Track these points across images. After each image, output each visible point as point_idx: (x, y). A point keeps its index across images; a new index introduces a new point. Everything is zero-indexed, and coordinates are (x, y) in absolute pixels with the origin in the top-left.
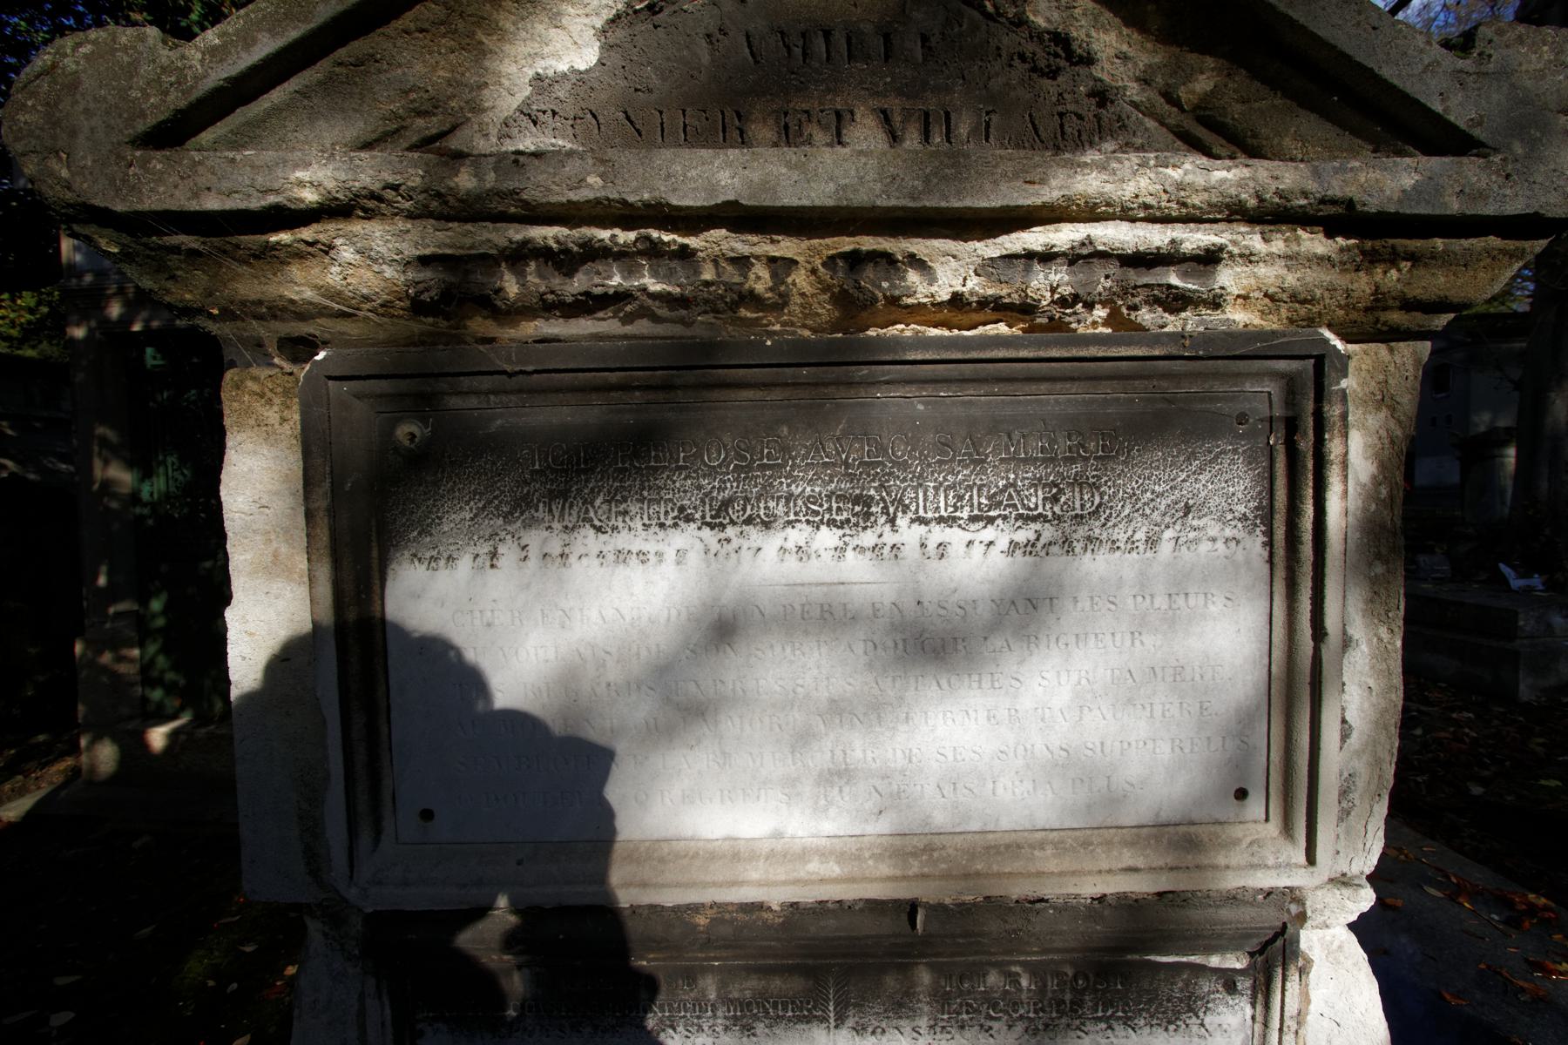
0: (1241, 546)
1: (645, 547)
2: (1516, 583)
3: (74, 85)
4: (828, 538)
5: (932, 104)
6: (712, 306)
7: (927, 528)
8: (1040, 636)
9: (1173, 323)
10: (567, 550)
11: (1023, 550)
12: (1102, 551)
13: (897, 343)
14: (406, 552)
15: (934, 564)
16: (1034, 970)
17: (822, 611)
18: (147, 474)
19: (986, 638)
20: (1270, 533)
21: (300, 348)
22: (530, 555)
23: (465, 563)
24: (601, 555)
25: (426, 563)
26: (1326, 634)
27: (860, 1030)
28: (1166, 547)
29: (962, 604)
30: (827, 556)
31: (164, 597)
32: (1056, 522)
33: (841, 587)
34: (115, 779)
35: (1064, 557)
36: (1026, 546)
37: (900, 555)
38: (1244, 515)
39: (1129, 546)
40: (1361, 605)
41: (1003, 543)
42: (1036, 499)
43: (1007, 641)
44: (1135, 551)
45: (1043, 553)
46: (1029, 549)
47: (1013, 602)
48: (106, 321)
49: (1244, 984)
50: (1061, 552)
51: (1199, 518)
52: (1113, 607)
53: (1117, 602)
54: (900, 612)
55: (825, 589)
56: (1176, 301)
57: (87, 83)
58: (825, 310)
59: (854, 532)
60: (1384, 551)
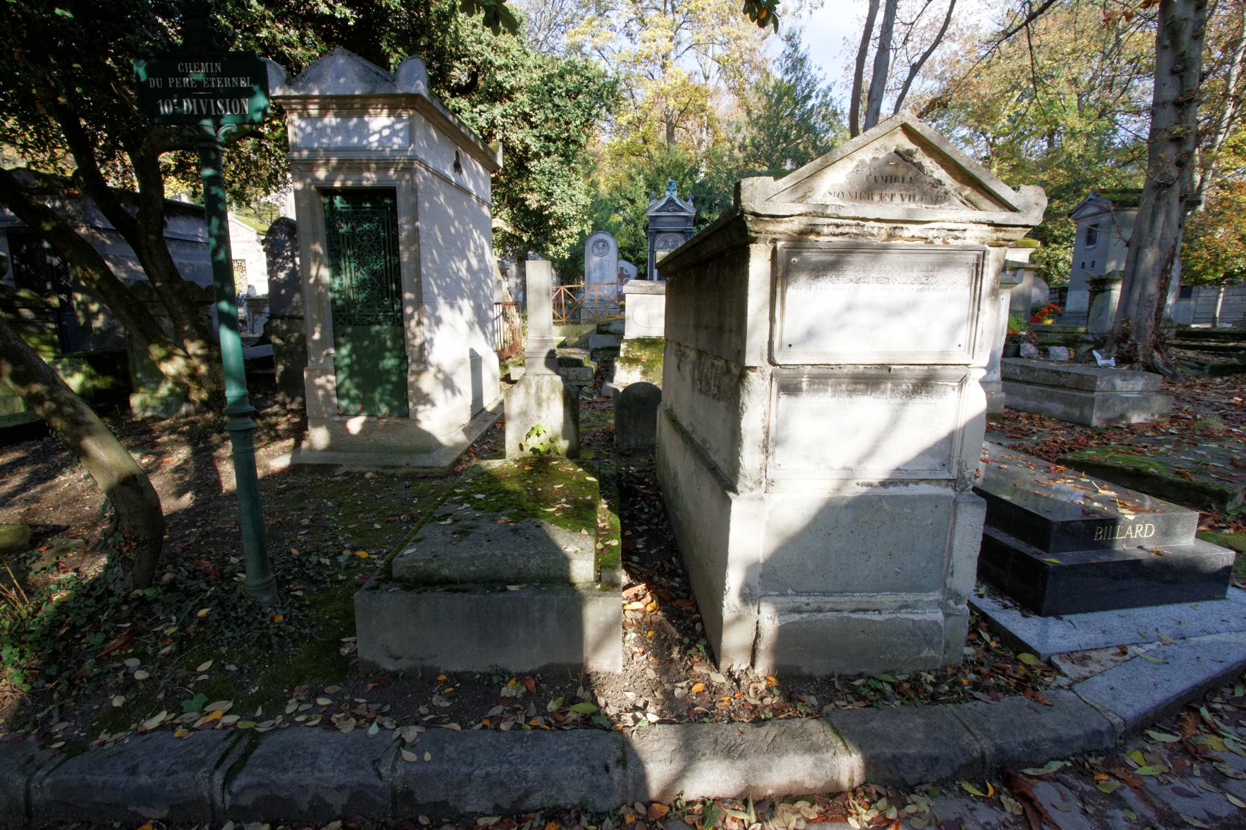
2: (1101, 362)
3: (756, 189)
5: (911, 192)
13: (897, 245)
18: (336, 271)
31: (349, 346)
34: (330, 448)
49: (957, 389)
56: (957, 238)
57: (759, 188)
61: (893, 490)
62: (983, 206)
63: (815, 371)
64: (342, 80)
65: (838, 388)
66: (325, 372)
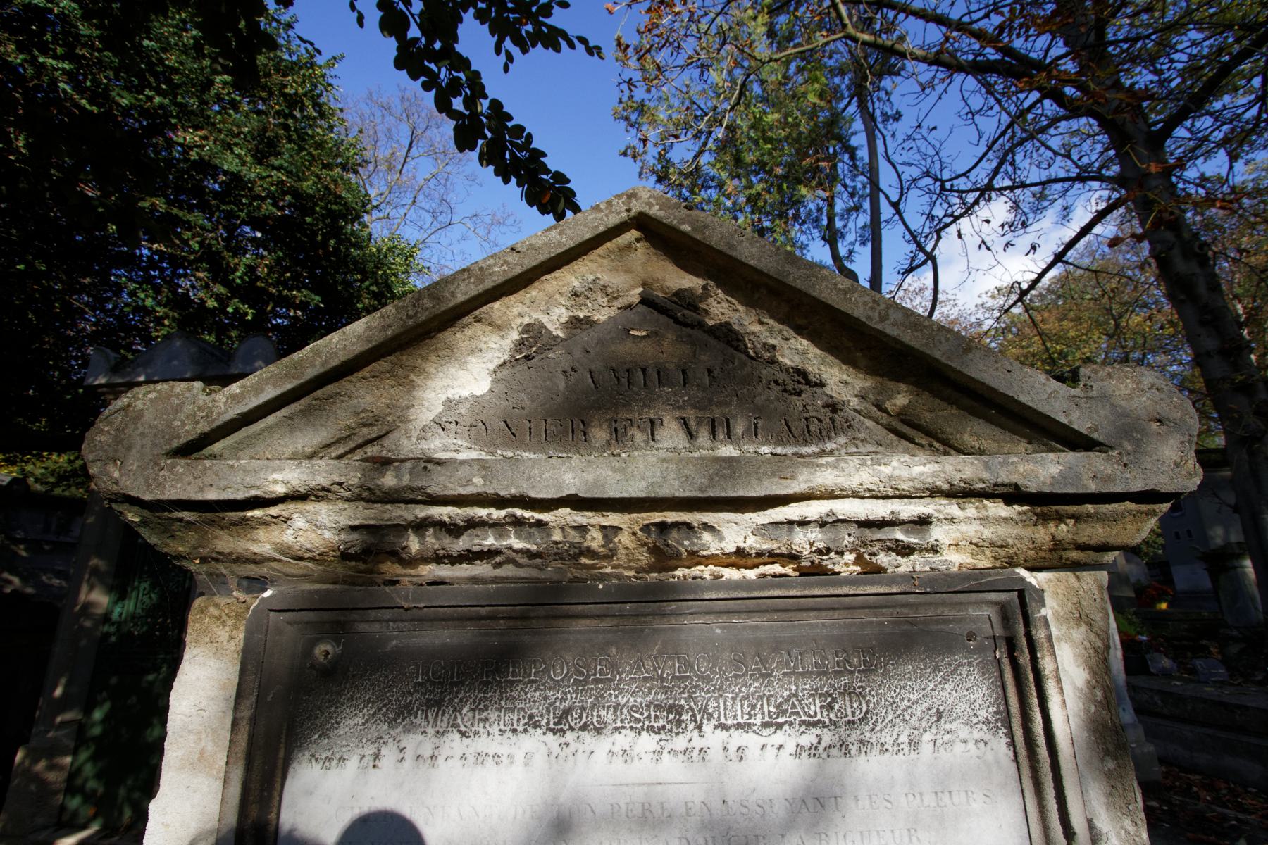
0: (989, 747)
1: (500, 750)
3: (139, 416)
4: (648, 742)
6: (560, 556)
7: (728, 734)
8: (829, 833)
9: (905, 565)
10: (436, 753)
11: (807, 752)
12: (874, 753)
14: (307, 753)
15: (735, 765)
17: (643, 809)
18: (122, 596)
19: (783, 836)
20: (1010, 735)
21: (255, 584)
22: (406, 756)
23: (353, 763)
24: (463, 757)
25: (321, 763)
26: (1075, 834)
28: (926, 748)
29: (760, 802)
30: (647, 758)
32: (833, 727)
33: (659, 787)
35: (843, 759)
36: (810, 749)
37: (707, 758)
38: (987, 718)
39: (896, 748)
40: (1103, 799)
41: (790, 747)
42: (815, 707)
43: (801, 837)
44: (902, 752)
45: (824, 756)
46: (813, 751)
47: (804, 801)
50: (839, 754)
51: (950, 722)
52: (889, 805)
53: (891, 799)
54: (709, 810)
55: (645, 788)
56: (905, 550)
57: (148, 417)
58: (644, 557)
59: (668, 737)
60: (1111, 748)
62: (970, 440)
64: (175, 362)
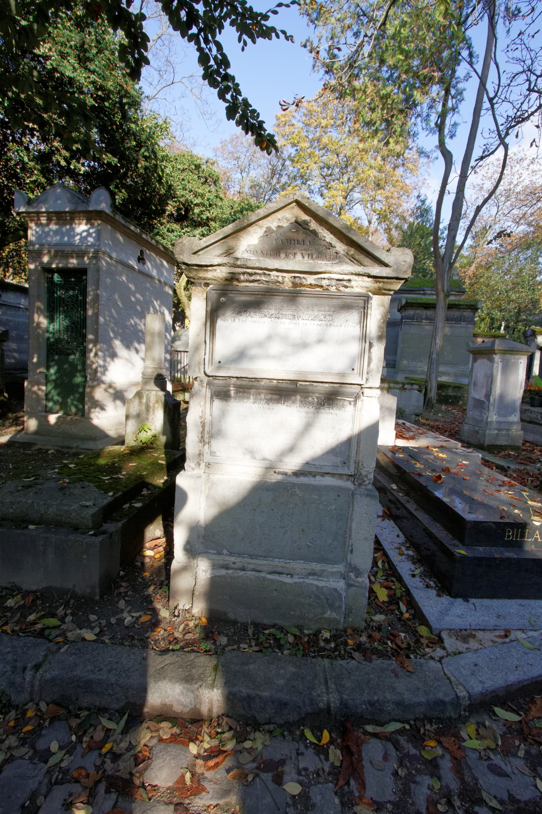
3: (184, 245)
4: (288, 321)
5: (310, 252)
6: (273, 283)
9: (347, 290)
13: (301, 290)
16: (317, 398)
18: (51, 320)
21: (207, 285)
23: (230, 321)
27: (287, 406)
28: (343, 327)
31: (56, 368)
34: (36, 433)
42: (322, 317)
48: (42, 263)
49: (352, 403)
56: (346, 287)
57: (187, 245)
58: (290, 285)
61: (303, 480)
62: (366, 263)
63: (239, 382)
64: (59, 202)
65: (259, 397)
66: (39, 383)
